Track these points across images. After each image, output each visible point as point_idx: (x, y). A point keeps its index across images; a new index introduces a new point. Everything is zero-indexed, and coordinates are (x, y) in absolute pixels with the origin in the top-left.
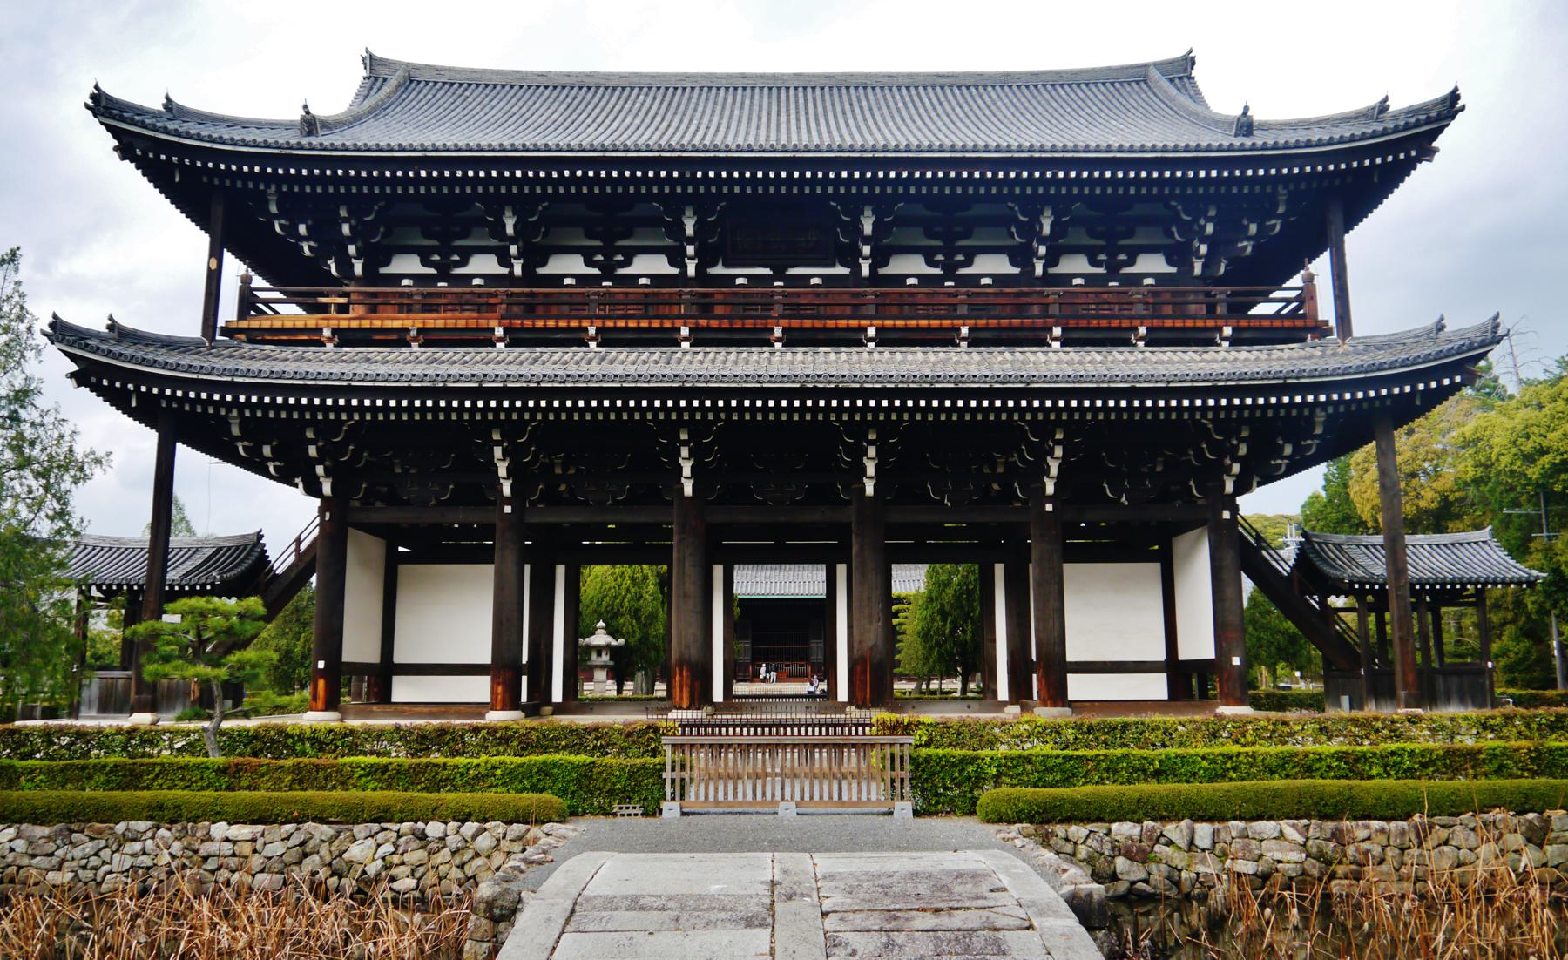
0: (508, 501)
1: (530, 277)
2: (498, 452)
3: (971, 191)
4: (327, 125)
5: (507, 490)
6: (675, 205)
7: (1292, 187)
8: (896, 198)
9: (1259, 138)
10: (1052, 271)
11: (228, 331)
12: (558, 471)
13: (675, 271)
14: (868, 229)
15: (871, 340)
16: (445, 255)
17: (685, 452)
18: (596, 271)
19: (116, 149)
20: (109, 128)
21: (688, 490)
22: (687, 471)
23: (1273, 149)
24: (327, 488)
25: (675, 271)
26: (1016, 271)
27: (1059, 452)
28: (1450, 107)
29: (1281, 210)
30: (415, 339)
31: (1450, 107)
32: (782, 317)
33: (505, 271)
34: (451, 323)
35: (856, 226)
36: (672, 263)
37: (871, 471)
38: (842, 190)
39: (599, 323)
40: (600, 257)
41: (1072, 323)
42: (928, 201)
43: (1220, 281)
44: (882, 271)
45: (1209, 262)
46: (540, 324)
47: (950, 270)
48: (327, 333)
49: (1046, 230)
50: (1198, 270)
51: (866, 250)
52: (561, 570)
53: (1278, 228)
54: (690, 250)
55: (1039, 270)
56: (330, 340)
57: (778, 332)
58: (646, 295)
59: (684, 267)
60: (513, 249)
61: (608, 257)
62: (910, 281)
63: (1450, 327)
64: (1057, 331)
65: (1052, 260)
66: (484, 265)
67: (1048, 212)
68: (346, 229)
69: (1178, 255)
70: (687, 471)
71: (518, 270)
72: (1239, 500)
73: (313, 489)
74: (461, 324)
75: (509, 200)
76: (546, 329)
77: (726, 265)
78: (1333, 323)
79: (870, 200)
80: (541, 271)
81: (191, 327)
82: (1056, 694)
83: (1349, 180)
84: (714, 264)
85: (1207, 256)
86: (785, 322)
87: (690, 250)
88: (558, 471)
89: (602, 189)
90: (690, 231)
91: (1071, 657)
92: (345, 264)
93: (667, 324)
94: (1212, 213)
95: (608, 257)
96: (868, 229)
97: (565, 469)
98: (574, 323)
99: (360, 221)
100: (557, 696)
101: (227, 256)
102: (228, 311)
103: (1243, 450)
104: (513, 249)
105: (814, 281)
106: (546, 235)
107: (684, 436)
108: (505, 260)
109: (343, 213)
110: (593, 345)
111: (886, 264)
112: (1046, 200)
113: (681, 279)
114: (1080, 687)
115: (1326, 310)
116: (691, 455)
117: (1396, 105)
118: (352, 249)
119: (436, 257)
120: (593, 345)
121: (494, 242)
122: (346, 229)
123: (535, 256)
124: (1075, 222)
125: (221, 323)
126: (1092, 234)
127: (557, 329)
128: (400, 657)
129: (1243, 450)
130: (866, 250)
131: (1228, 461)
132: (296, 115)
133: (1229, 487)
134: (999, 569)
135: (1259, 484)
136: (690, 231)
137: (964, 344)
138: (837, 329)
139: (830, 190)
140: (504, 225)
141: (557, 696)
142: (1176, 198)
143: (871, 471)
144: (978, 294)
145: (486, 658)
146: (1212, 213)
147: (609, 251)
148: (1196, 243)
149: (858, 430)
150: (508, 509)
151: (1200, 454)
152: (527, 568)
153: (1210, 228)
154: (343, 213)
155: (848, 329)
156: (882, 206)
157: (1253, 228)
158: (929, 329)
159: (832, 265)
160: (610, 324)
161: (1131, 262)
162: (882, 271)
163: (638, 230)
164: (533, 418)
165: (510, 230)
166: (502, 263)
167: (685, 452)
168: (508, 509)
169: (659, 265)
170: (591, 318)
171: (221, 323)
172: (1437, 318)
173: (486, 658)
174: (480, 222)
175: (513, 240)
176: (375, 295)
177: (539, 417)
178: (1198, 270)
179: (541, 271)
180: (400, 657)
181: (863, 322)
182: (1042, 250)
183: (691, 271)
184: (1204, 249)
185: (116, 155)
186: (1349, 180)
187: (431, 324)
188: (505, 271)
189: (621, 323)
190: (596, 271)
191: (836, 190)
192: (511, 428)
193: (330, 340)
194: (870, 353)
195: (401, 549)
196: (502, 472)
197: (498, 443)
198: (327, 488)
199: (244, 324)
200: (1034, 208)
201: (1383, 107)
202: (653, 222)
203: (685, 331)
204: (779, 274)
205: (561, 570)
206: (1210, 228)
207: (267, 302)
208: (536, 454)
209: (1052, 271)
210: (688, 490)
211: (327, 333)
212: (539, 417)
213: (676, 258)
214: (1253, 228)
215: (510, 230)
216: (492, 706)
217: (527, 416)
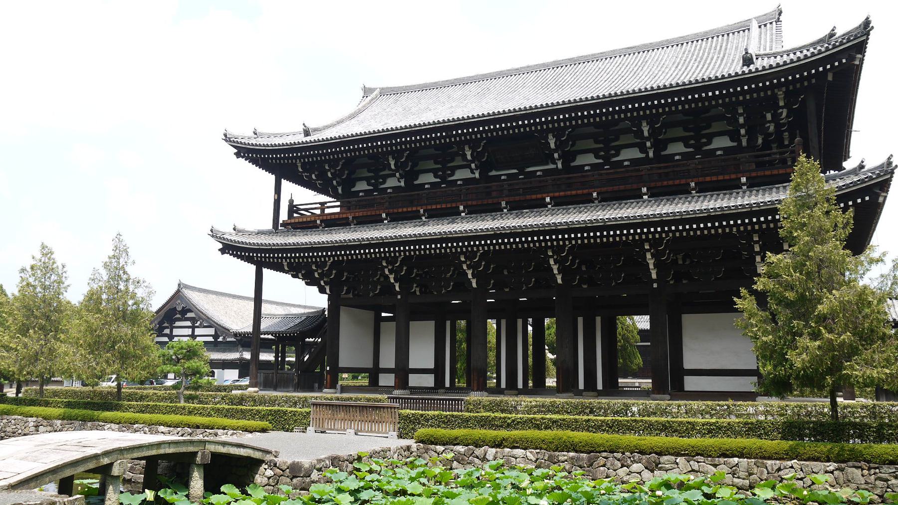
0: (398, 293)
1: (658, 157)
2: (649, 256)
3: (418, 145)
4: (315, 130)
5: (654, 276)
6: (637, 122)
8: (566, 128)
9: (759, 64)
11: (284, 224)
12: (680, 262)
13: (643, 155)
15: (549, 204)
16: (376, 180)
18: (601, 161)
23: (776, 67)
24: (328, 291)
25: (735, 144)
28: (866, 27)
30: (353, 222)
31: (866, 27)
32: (506, 196)
34: (365, 214)
35: (464, 156)
38: (539, 128)
39: (425, 207)
40: (692, 142)
41: (653, 185)
42: (436, 147)
45: (752, 139)
46: (400, 210)
47: (698, 148)
48: (318, 222)
52: (448, 323)
54: (743, 131)
56: (321, 225)
57: (503, 204)
58: (540, 182)
60: (648, 144)
61: (444, 172)
62: (586, 168)
63: (869, 165)
64: (644, 190)
66: (461, 175)
68: (329, 175)
71: (651, 154)
73: (322, 291)
74: (369, 213)
75: (467, 142)
76: (403, 212)
77: (497, 170)
79: (645, 117)
81: (269, 226)
82: (402, 382)
83: (814, 81)
84: (491, 171)
86: (507, 199)
87: (743, 131)
88: (680, 262)
89: (440, 141)
93: (454, 205)
95: (444, 172)
97: (684, 261)
98: (414, 209)
100: (447, 385)
102: (284, 216)
104: (648, 144)
105: (538, 173)
107: (756, 238)
108: (643, 149)
110: (423, 218)
113: (646, 161)
114: (691, 383)
117: (839, 32)
119: (602, 153)
120: (423, 218)
122: (329, 175)
123: (660, 145)
125: (281, 222)
126: (686, 130)
127: (408, 212)
128: (381, 366)
134: (598, 319)
137: (596, 202)
138: (532, 200)
139: (533, 128)
141: (447, 385)
142: (720, 105)
144: (583, 176)
147: (376, 178)
150: (399, 297)
152: (598, 319)
155: (537, 199)
157: (769, 116)
158: (577, 195)
159: (547, 164)
160: (429, 207)
161: (709, 143)
165: (646, 134)
166: (641, 152)
168: (655, 285)
169: (634, 153)
170: (421, 206)
171: (281, 222)
172: (859, 162)
174: (458, 155)
175: (648, 139)
177: (671, 235)
180: (381, 366)
181: (739, 175)
183: (744, 143)
186: (814, 81)
187: (357, 214)
189: (434, 207)
190: (601, 161)
191: (536, 128)
192: (391, 261)
193: (321, 225)
195: (383, 314)
196: (556, 272)
197: (552, 257)
198: (328, 291)
199: (293, 221)
201: (831, 35)
202: (627, 131)
203: (548, 200)
204: (521, 171)
205: (448, 323)
207: (306, 210)
211: (318, 222)
212: (671, 235)
213: (734, 136)
215: (646, 134)
216: (394, 388)
217: (664, 235)
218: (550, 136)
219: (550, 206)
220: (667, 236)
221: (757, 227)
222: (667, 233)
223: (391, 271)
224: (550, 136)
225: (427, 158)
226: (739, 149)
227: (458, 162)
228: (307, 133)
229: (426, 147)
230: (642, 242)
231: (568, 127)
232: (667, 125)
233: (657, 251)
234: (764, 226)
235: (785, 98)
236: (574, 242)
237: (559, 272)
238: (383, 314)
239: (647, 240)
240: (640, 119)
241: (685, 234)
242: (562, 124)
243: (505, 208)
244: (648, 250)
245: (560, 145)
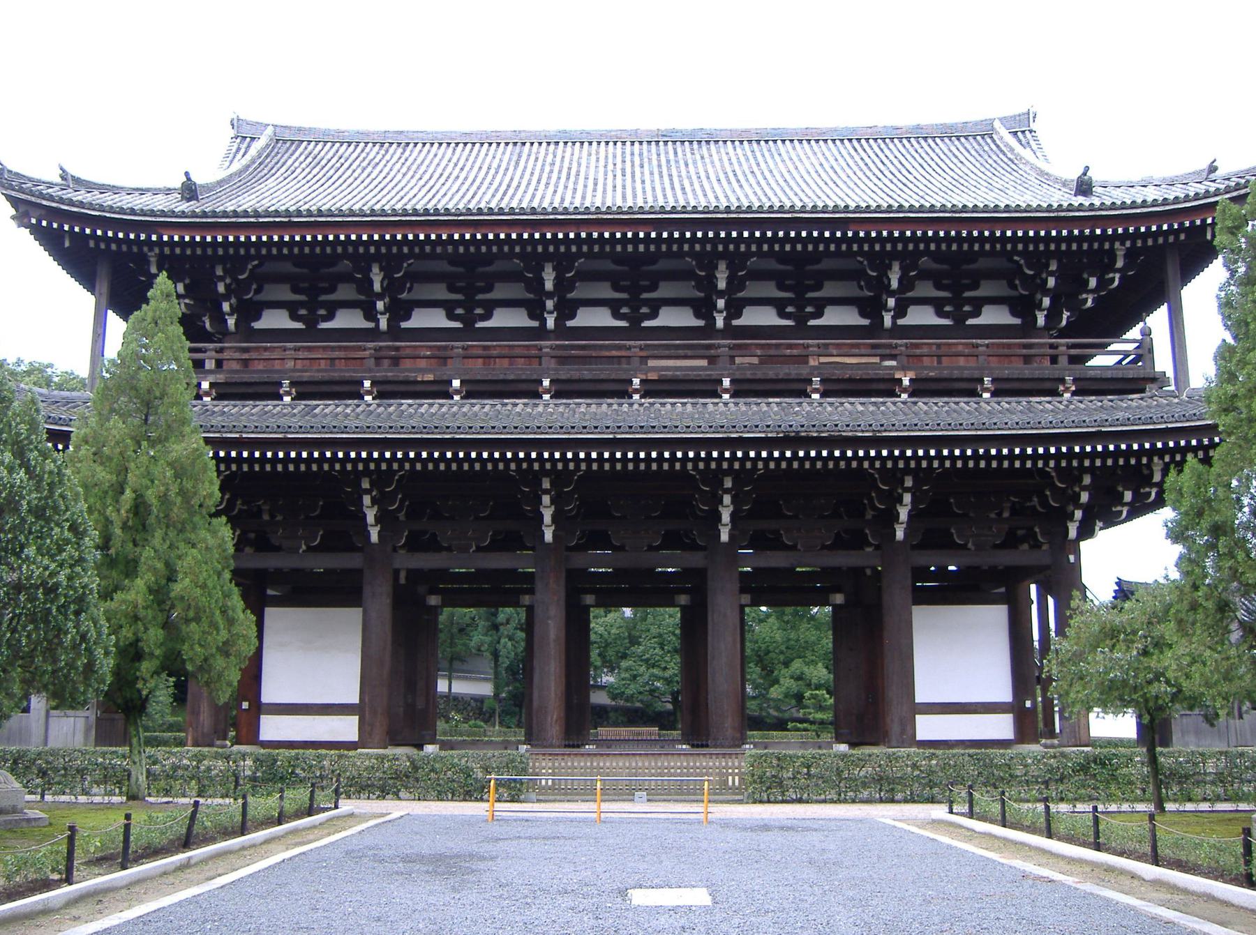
1: (395, 332)
2: (367, 500)
7: (1128, 244)
8: (749, 254)
10: (900, 322)
13: (535, 324)
14: (722, 285)
17: (546, 499)
19: (13, 218)
20: (8, 198)
21: (548, 536)
22: (547, 519)
25: (535, 324)
26: (866, 322)
27: (907, 498)
29: (1120, 264)
33: (371, 325)
35: (712, 279)
36: (532, 316)
37: (726, 517)
40: (460, 311)
43: (1063, 334)
44: (735, 322)
45: (1053, 315)
49: (895, 284)
50: (1041, 321)
51: (721, 303)
53: (1116, 283)
54: (550, 304)
55: (888, 320)
59: (543, 322)
60: (380, 305)
65: (900, 311)
67: (896, 267)
68: (221, 288)
69: (1023, 307)
70: (547, 519)
71: (383, 324)
72: (1085, 546)
78: (1170, 374)
79: (724, 255)
80: (404, 325)
83: (1182, 237)
85: (1048, 310)
87: (550, 304)
90: (549, 286)
91: (919, 698)
92: (220, 319)
94: (1053, 267)
96: (722, 285)
99: (235, 280)
101: (111, 314)
103: (1085, 497)
106: (410, 290)
108: (370, 314)
109: (219, 272)
111: (739, 315)
112: (894, 255)
115: (1163, 362)
116: (552, 502)
118: (226, 307)
121: (363, 297)
122: (221, 288)
123: (400, 310)
124: (925, 275)
129: (1085, 497)
130: (721, 303)
131: (1071, 508)
132: (177, 182)
133: (1073, 533)
135: (1101, 529)
136: (549, 286)
140: (371, 282)
142: (1019, 254)
143: (726, 517)
145: (354, 699)
146: (1053, 267)
148: (1038, 296)
149: (714, 478)
151: (1044, 502)
153: (1051, 282)
154: (219, 272)
156: (736, 262)
157: (1093, 282)
162: (735, 322)
163: (497, 285)
164: (401, 467)
167: (546, 499)
173: (354, 699)
174: (346, 278)
175: (380, 296)
176: (246, 350)
177: (407, 466)
178: (1041, 321)
179: (404, 325)
182: (891, 302)
183: (550, 323)
184: (1046, 302)
185: (13, 224)
186: (1182, 237)
188: (371, 325)
194: (726, 404)
200: (881, 262)
206: (1051, 282)
208: (402, 501)
209: (900, 322)
210: (548, 536)
212: (407, 466)
213: (536, 311)
214: (1093, 282)
215: (377, 287)
217: (395, 466)
218: (375, 269)
219: (457, 398)
220: (401, 467)
221: (548, 466)
222: (401, 462)
223: (374, 501)
224: (375, 269)
225: (279, 279)
226: (541, 333)
227: (345, 292)
228: (190, 191)
229: (280, 257)
230: (359, 476)
231: (253, 258)
232: (417, 277)
233: (382, 493)
234: (924, 464)
235: (1125, 256)
236: (234, 467)
237: (378, 520)
238: (270, 592)
239: (367, 472)
240: (368, 260)
241: (807, 465)
242: (743, 248)
243: (288, 393)
244: (368, 492)
245: (392, 288)
